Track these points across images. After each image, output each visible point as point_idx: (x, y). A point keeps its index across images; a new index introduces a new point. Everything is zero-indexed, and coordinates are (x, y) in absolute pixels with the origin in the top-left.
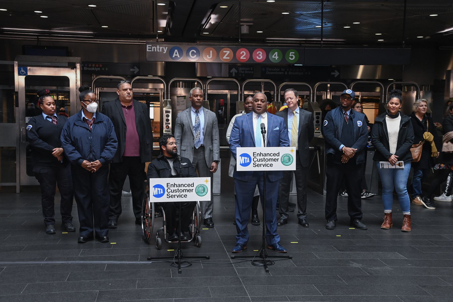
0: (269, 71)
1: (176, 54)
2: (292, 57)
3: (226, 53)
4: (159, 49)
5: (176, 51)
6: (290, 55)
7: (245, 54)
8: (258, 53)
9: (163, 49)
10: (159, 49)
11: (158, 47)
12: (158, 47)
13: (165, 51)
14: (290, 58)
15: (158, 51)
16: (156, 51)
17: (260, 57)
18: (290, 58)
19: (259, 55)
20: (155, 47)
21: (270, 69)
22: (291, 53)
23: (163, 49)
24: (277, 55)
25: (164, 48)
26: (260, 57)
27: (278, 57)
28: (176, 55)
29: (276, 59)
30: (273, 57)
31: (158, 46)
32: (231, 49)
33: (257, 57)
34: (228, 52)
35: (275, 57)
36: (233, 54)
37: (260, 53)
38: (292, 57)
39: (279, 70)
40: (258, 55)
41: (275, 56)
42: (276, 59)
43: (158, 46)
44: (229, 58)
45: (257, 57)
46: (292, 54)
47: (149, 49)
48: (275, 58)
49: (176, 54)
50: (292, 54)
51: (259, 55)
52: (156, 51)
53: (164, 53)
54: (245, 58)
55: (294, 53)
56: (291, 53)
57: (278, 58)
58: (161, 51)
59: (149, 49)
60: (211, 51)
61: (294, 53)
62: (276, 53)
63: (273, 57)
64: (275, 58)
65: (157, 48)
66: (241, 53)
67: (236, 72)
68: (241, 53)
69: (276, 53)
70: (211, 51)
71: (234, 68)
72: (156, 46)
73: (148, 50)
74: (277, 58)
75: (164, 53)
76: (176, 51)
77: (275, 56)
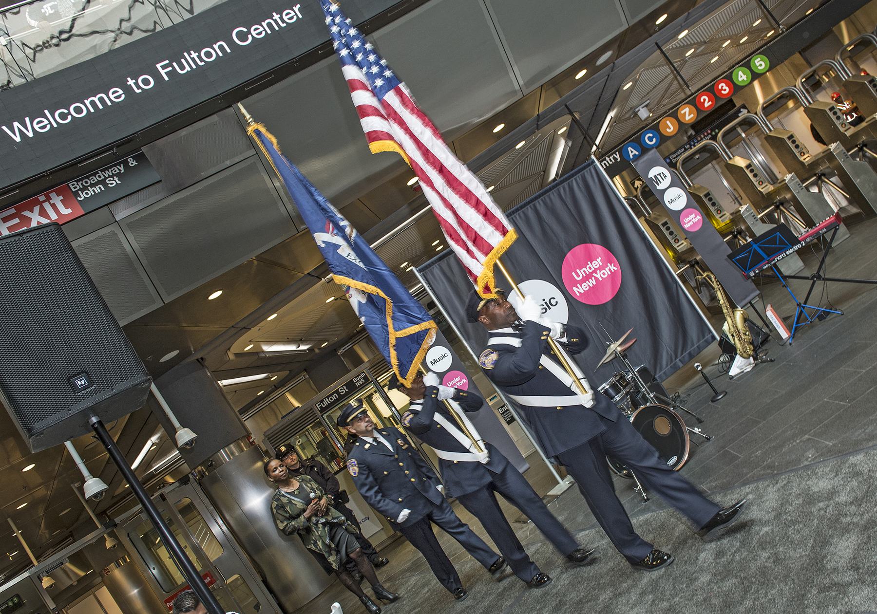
0: (675, 158)
1: (632, 152)
2: (761, 65)
3: (685, 113)
4: (611, 161)
5: (630, 149)
6: (758, 65)
7: (707, 99)
8: (720, 88)
9: (614, 158)
10: (611, 161)
11: (608, 159)
12: (608, 159)
13: (618, 157)
14: (759, 68)
15: (611, 163)
16: (608, 165)
17: (725, 90)
18: (759, 68)
19: (723, 88)
20: (605, 162)
21: (674, 156)
22: (756, 61)
23: (614, 158)
24: (742, 75)
25: (614, 155)
26: (725, 90)
28: (633, 154)
29: (745, 79)
30: (740, 79)
31: (607, 158)
33: (723, 92)
34: (687, 110)
36: (694, 108)
37: (722, 87)
38: (761, 65)
39: (683, 150)
40: (722, 89)
41: (741, 77)
42: (745, 79)
43: (607, 158)
44: (692, 115)
45: (723, 92)
49: (632, 152)
51: (723, 88)
52: (608, 165)
53: (618, 160)
54: (710, 103)
56: (756, 61)
58: (613, 161)
60: (668, 122)
61: (759, 59)
62: (740, 73)
63: (740, 79)
65: (607, 162)
66: (702, 100)
67: (641, 183)
68: (702, 100)
69: (740, 73)
70: (668, 122)
71: (636, 181)
72: (605, 159)
74: (744, 77)
75: (618, 160)
76: (630, 149)
77: (741, 77)
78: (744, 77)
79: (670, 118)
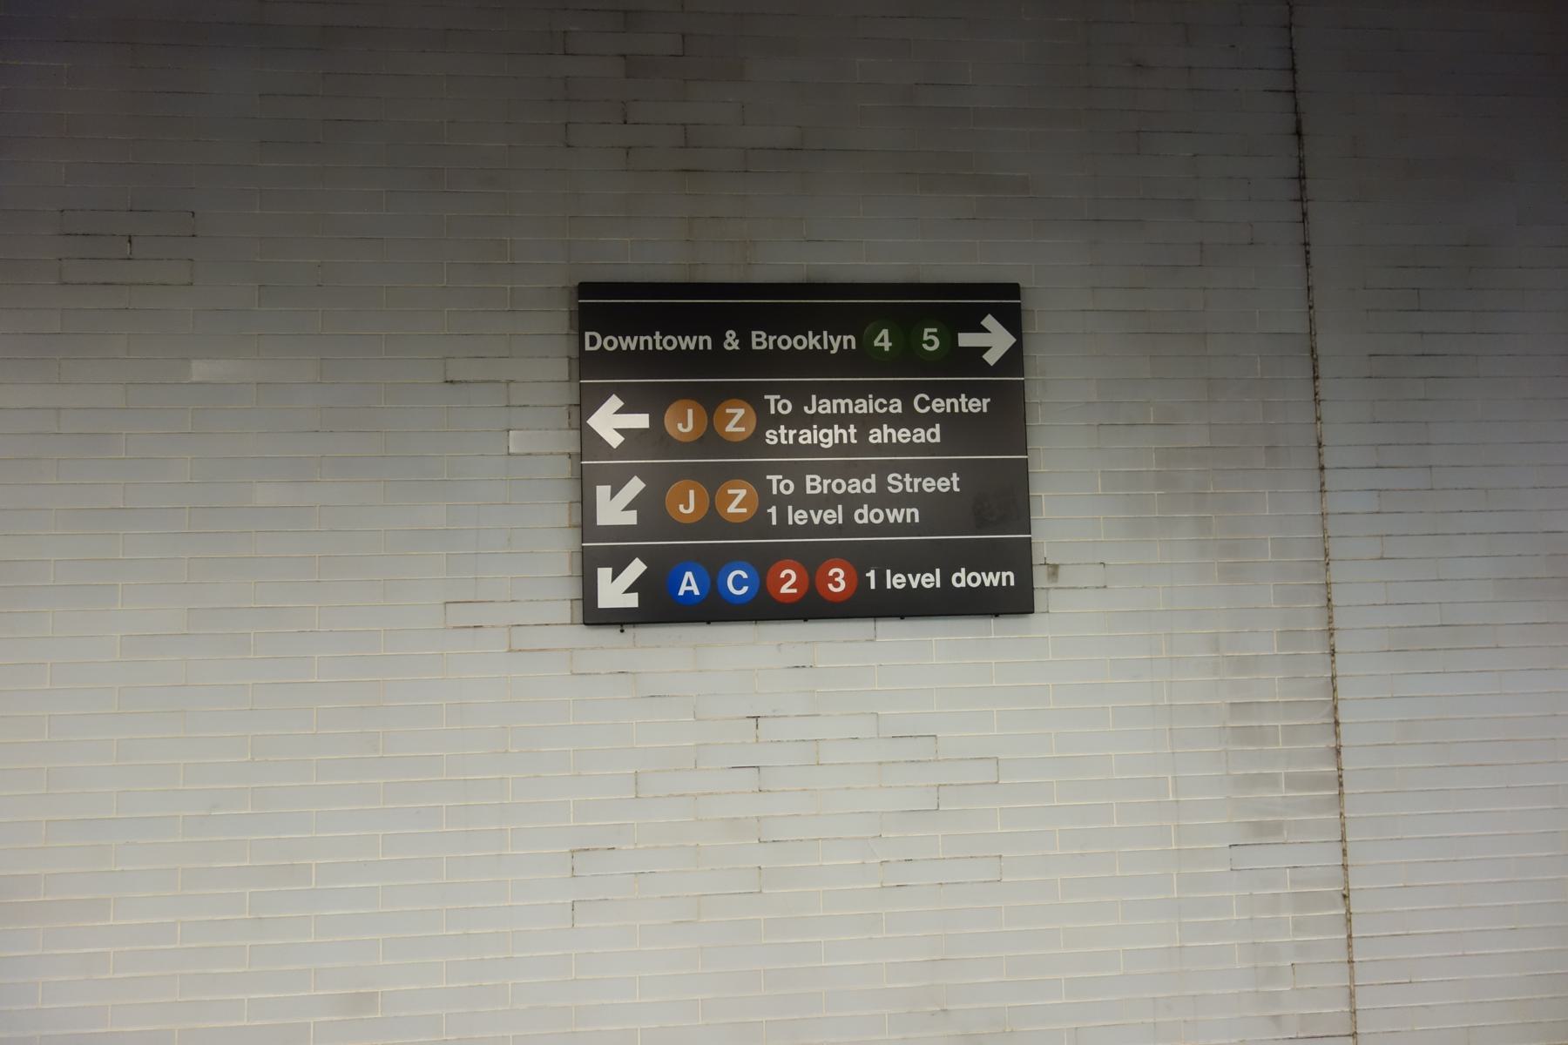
2: (931, 343)
6: (926, 338)
14: (925, 346)
18: (925, 346)
22: (927, 330)
24: (886, 339)
27: (891, 344)
29: (887, 349)
30: (876, 343)
35: (881, 344)
38: (931, 343)
42: (887, 349)
46: (929, 334)
48: (883, 347)
50: (929, 334)
55: (935, 330)
56: (927, 330)
57: (890, 347)
61: (935, 330)
62: (885, 333)
63: (876, 343)
64: (883, 347)
69: (885, 333)
74: (887, 345)
77: (882, 340)
78: (887, 345)
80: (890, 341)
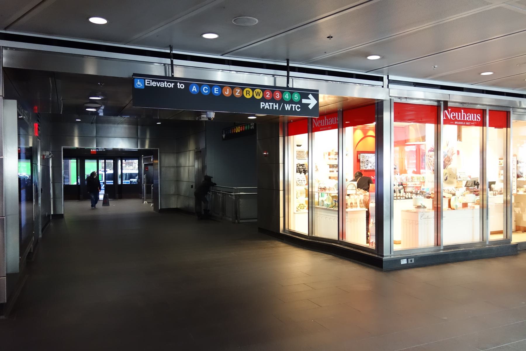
2: (296, 98)
15: (166, 86)
17: (278, 96)
18: (295, 98)
26: (278, 96)
30: (285, 97)
32: (241, 88)
33: (276, 96)
35: (286, 97)
38: (296, 98)
45: (276, 96)
47: (148, 84)
59: (148, 84)
63: (285, 97)
73: (146, 85)
74: (287, 97)
77: (286, 96)
78: (287, 97)
79: (230, 88)
80: (288, 96)
